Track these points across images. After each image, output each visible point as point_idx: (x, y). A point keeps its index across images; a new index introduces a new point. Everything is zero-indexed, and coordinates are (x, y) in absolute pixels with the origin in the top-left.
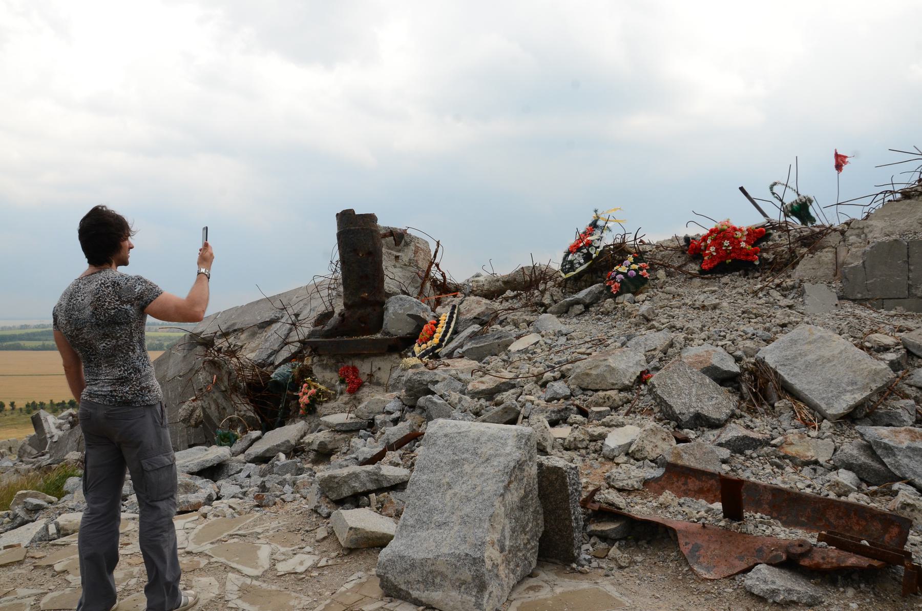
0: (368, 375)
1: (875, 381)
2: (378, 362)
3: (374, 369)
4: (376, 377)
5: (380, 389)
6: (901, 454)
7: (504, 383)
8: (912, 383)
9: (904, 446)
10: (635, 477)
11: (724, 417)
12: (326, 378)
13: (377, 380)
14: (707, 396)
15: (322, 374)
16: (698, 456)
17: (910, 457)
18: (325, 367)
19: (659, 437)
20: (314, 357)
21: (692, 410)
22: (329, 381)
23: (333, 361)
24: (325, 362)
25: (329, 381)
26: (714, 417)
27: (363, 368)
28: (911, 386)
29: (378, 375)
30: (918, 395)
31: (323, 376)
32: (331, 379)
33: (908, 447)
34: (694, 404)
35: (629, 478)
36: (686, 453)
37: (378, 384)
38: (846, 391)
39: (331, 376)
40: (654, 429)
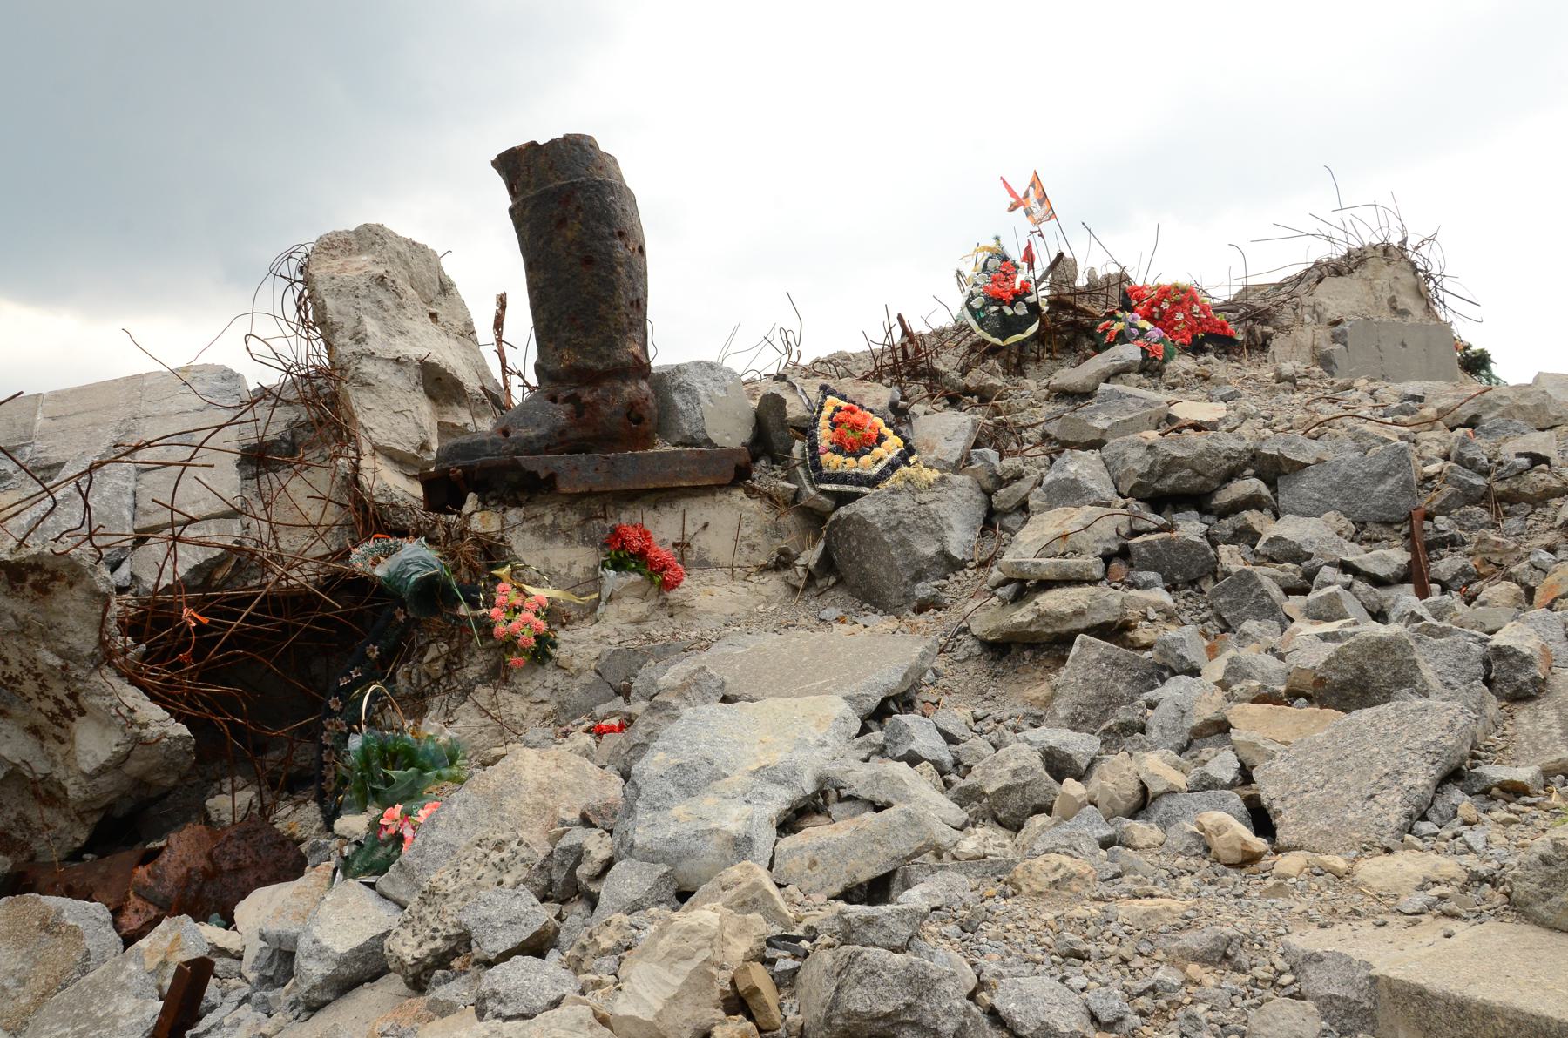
0: (675, 545)
2: (698, 512)
3: (690, 530)
4: (695, 548)
5: (719, 575)
12: (554, 565)
13: (699, 556)
15: (542, 555)
18: (550, 533)
20: (504, 510)
22: (564, 571)
23: (573, 517)
24: (548, 520)
25: (564, 571)
27: (660, 527)
29: (702, 542)
31: (546, 560)
32: (571, 565)
37: (703, 564)
39: (577, 558)
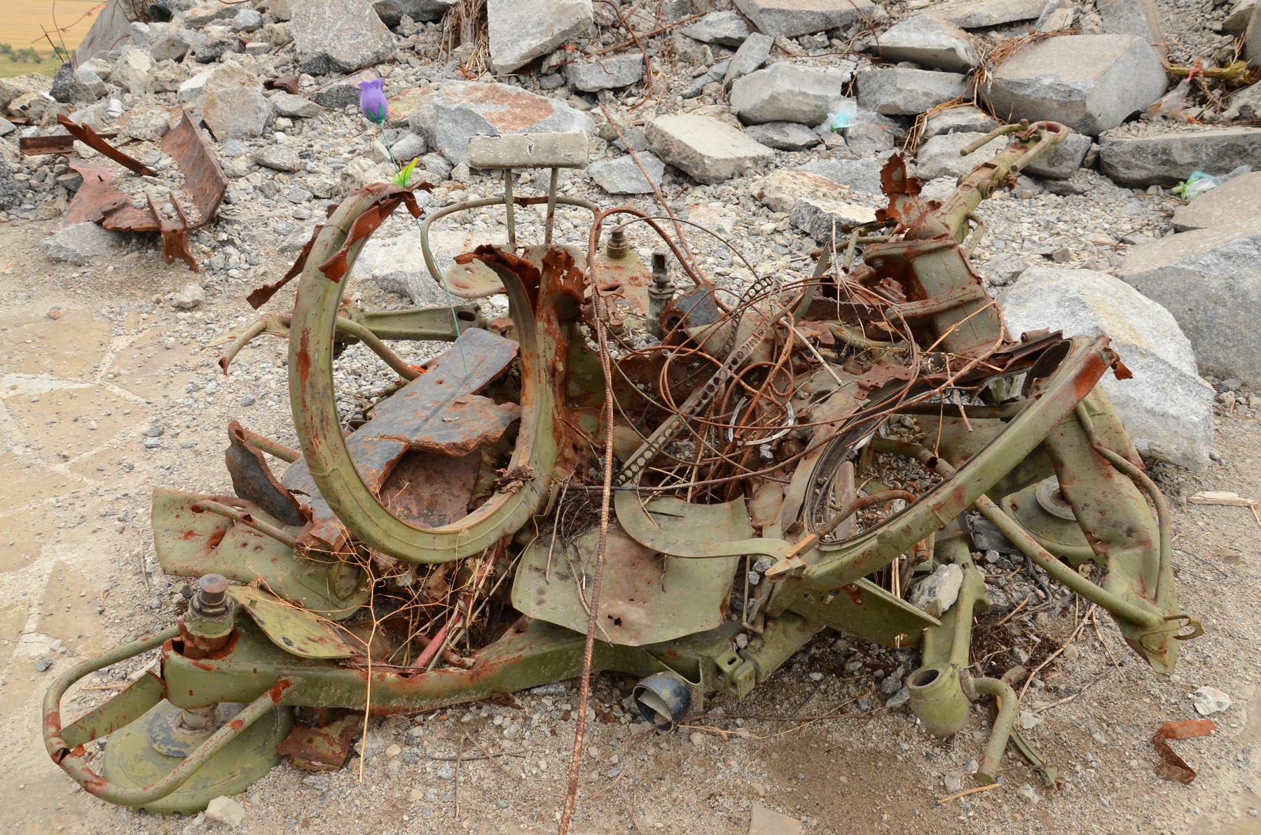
1: (560, 22)
6: (446, 116)
7: (228, 9)
8: (687, 33)
9: (454, 107)
10: (152, 125)
11: (355, 61)
14: (352, 32)
16: (234, 106)
17: (456, 122)
19: (237, 80)
21: (319, 50)
26: (343, 60)
28: (686, 36)
30: (689, 50)
33: (459, 109)
34: (326, 43)
35: (146, 126)
36: (222, 100)
38: (528, 34)
40: (229, 70)
